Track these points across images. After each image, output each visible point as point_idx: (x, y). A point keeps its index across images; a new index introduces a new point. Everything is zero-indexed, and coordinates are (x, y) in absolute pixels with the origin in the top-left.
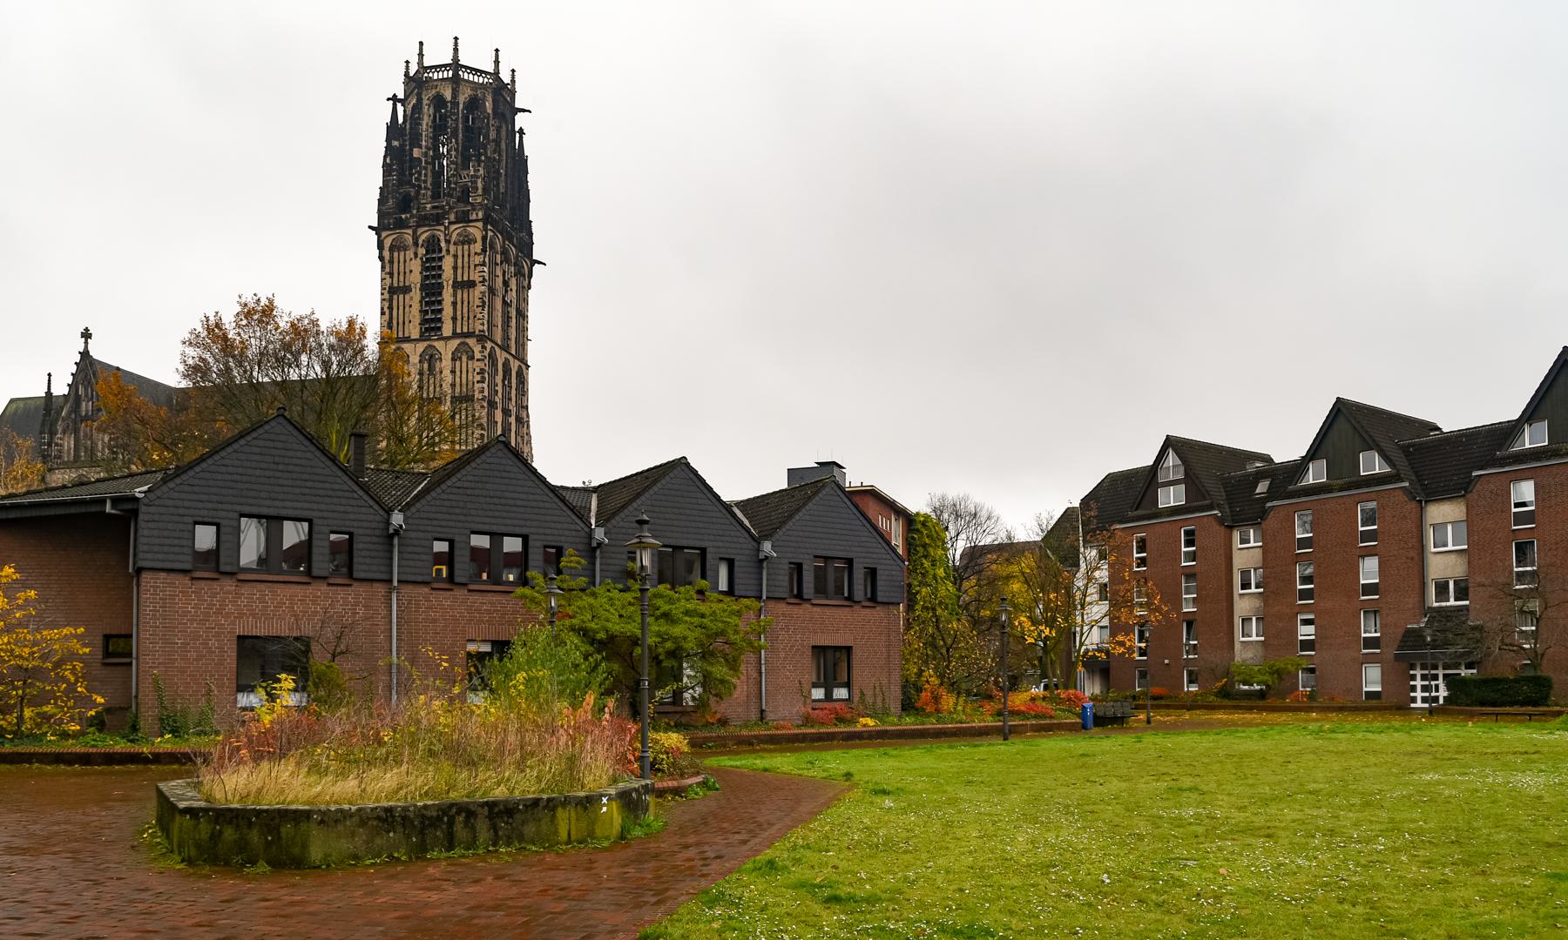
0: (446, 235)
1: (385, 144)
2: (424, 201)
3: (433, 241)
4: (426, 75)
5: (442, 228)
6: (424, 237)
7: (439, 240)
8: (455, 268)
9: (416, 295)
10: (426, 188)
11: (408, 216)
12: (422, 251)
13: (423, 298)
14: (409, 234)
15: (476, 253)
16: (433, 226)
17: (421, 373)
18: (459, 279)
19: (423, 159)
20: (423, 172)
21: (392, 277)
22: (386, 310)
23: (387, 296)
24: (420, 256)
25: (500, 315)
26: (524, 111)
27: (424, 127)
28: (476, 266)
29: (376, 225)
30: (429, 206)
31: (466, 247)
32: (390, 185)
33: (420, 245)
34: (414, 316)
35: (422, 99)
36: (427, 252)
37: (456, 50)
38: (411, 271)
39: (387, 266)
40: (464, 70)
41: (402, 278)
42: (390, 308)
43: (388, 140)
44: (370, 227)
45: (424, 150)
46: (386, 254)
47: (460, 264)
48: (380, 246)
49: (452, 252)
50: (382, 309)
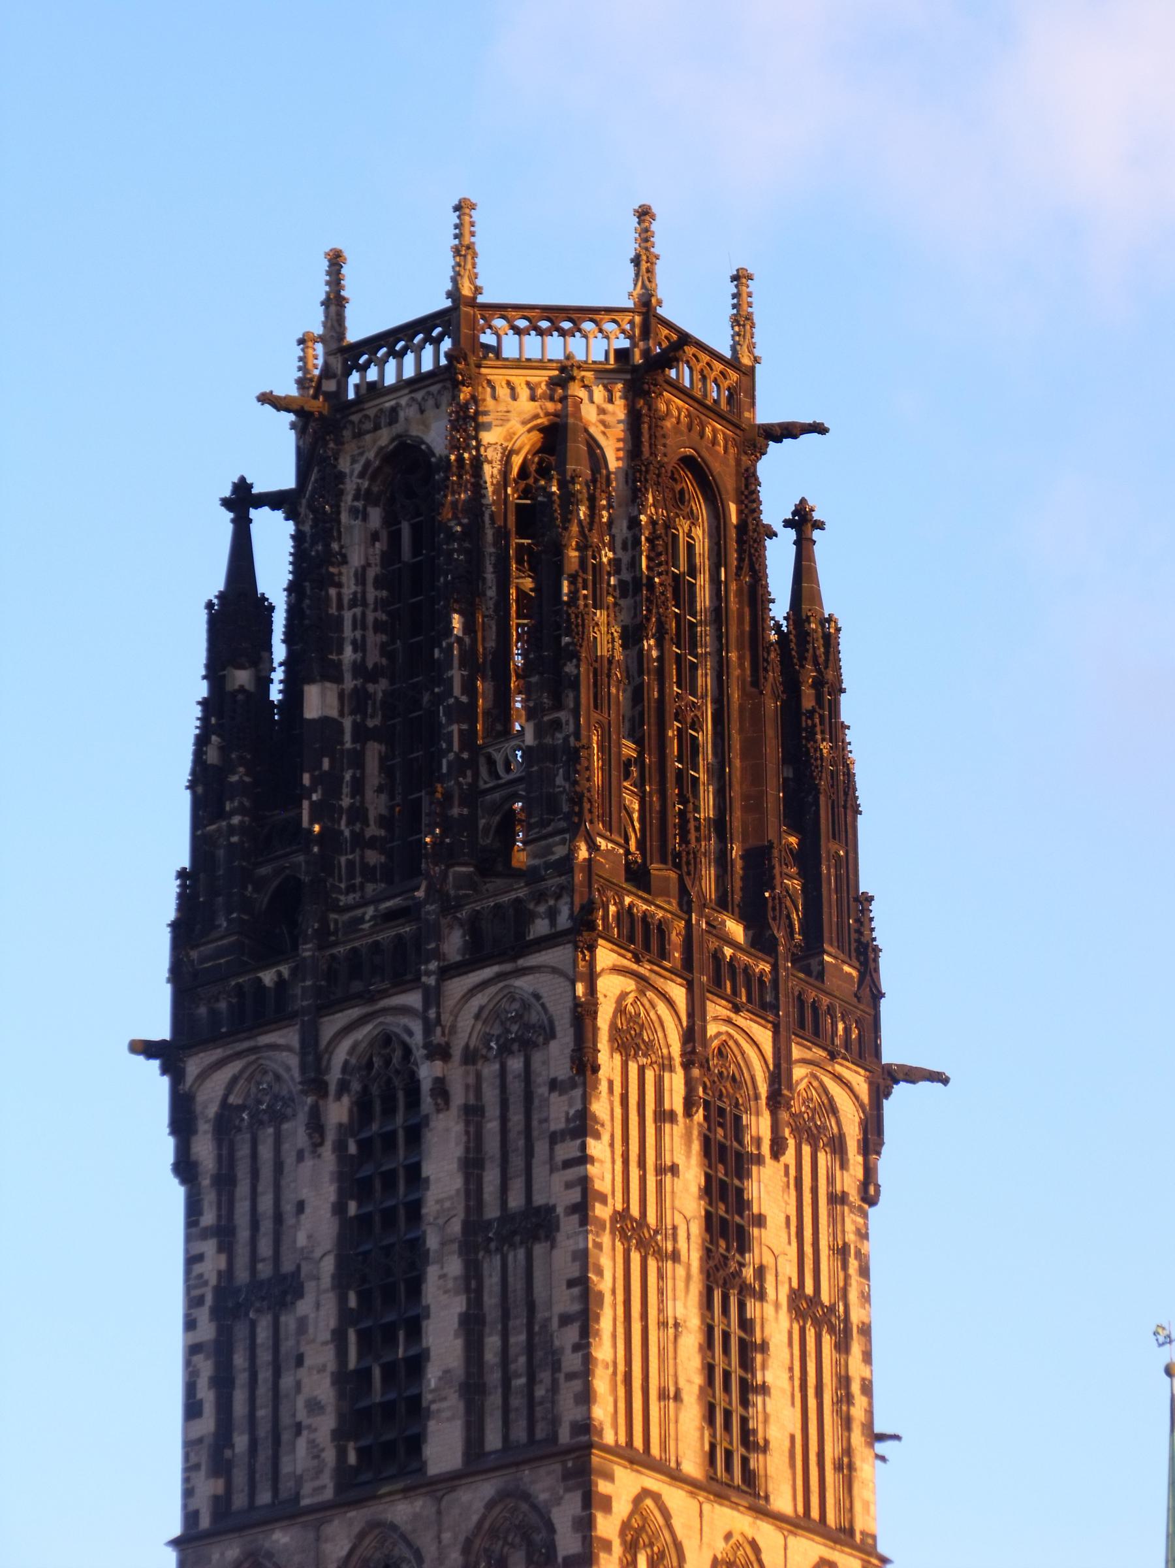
0: (428, 1030)
1: (202, 690)
2: (350, 899)
3: (388, 1062)
4: (354, 378)
5: (414, 999)
7: (407, 1051)
8: (472, 1165)
10: (359, 841)
11: (285, 970)
13: (346, 1317)
14: (288, 1048)
15: (554, 1085)
16: (384, 994)
18: (492, 1212)
19: (347, 723)
20: (348, 776)
21: (226, 1245)
22: (207, 1395)
23: (207, 1331)
24: (331, 1137)
25: (691, 1342)
27: (350, 588)
29: (161, 1029)
30: (370, 911)
31: (515, 1064)
32: (221, 853)
33: (332, 1088)
34: (314, 1407)
35: (340, 477)
36: (363, 1109)
37: (464, 252)
38: (300, 1207)
39: (209, 1198)
40: (499, 323)
41: (265, 1248)
42: (223, 1382)
43: (215, 671)
44: (146, 1049)
45: (349, 683)
46: (204, 1149)
47: (492, 1145)
49: (458, 1097)
50: (190, 1389)
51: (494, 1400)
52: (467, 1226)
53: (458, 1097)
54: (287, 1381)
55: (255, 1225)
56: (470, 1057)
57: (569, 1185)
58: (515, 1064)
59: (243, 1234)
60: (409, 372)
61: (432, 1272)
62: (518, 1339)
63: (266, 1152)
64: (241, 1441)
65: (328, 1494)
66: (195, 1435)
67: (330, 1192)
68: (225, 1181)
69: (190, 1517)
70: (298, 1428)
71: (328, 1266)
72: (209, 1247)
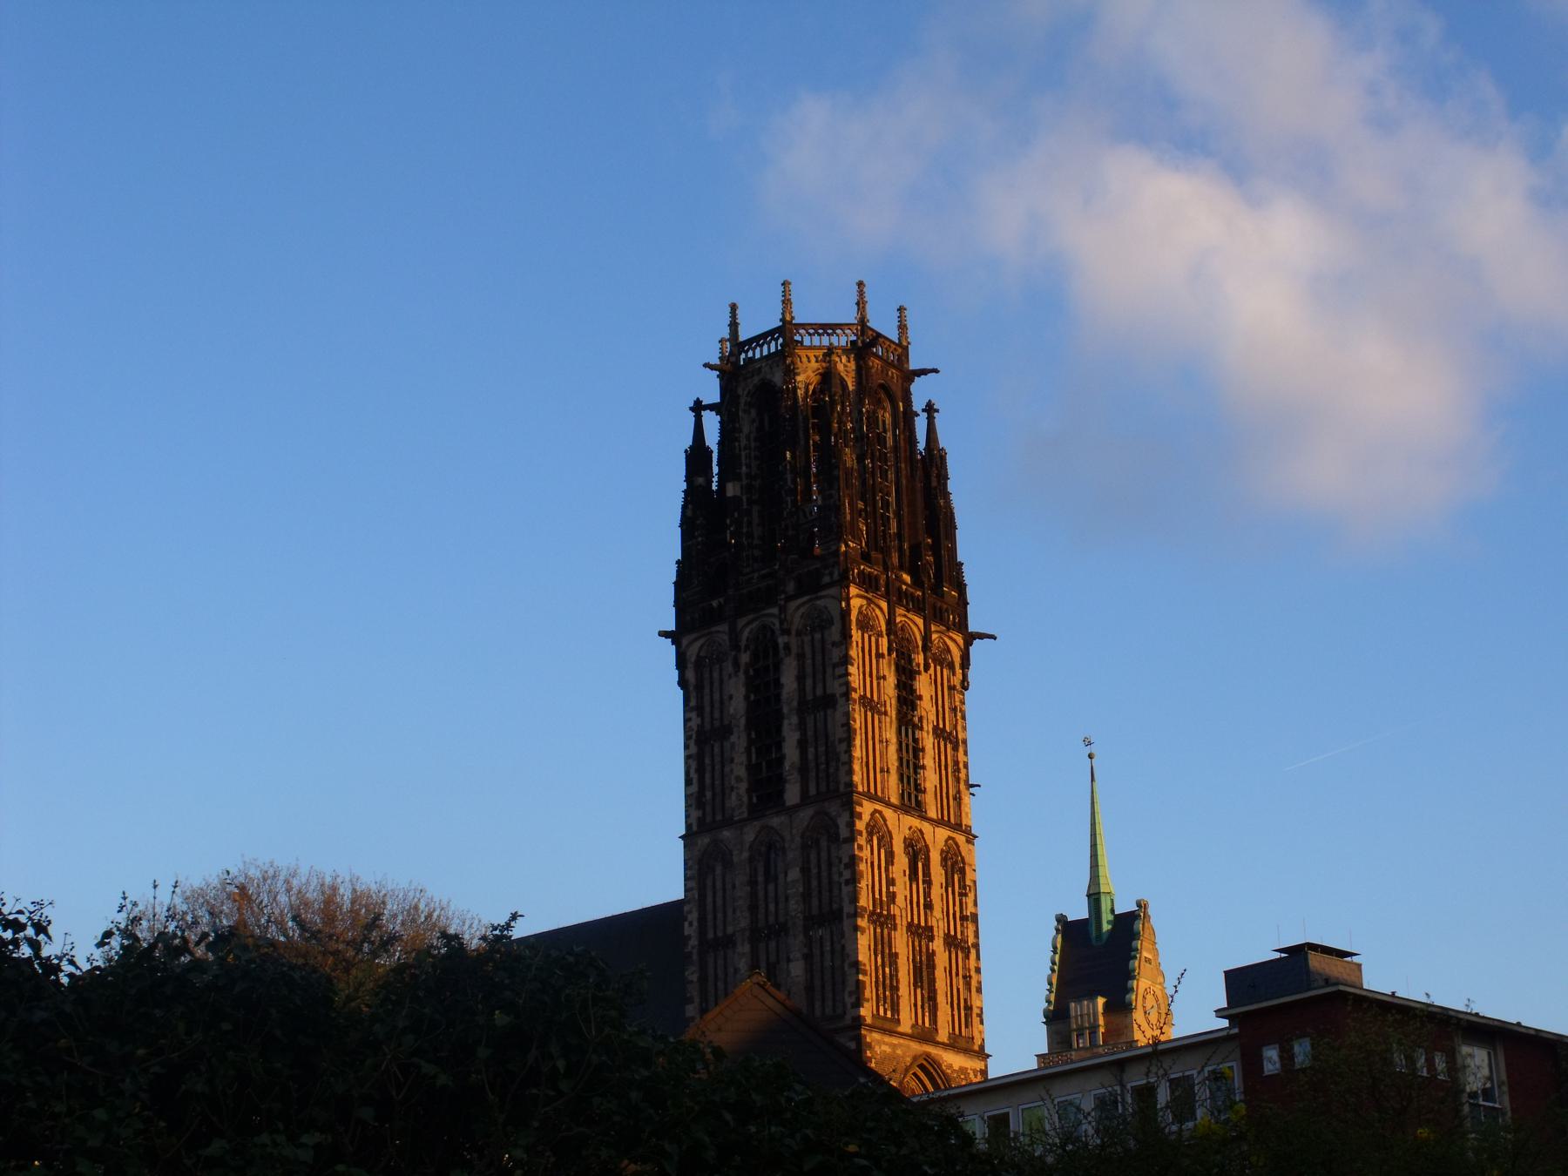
0: (781, 623)
1: (684, 486)
2: (748, 570)
4: (743, 356)
5: (775, 611)
6: (746, 633)
7: (773, 632)
8: (801, 678)
9: (739, 739)
11: (721, 600)
12: (745, 658)
13: (751, 742)
15: (834, 644)
17: (753, 883)
18: (810, 697)
20: (745, 519)
21: (701, 714)
22: (694, 776)
23: (693, 749)
25: (893, 748)
26: (924, 372)
27: (744, 442)
28: (835, 666)
29: (671, 626)
30: (756, 575)
31: (818, 636)
33: (743, 647)
34: (739, 779)
37: (786, 302)
38: (731, 697)
40: (802, 331)
41: (717, 715)
42: (701, 770)
43: (689, 478)
44: (664, 634)
45: (745, 482)
46: (690, 675)
47: (809, 670)
48: (681, 663)
49: (794, 650)
51: (813, 774)
52: (799, 704)
53: (794, 650)
54: (727, 769)
55: (712, 706)
56: (799, 634)
57: (841, 685)
58: (818, 636)
59: (707, 709)
60: (765, 352)
61: (786, 722)
62: (822, 749)
63: (716, 675)
64: (709, 794)
65: (745, 815)
66: (689, 793)
67: (743, 690)
68: (699, 687)
69: (688, 826)
70: (732, 789)
71: (743, 721)
72: (693, 715)
